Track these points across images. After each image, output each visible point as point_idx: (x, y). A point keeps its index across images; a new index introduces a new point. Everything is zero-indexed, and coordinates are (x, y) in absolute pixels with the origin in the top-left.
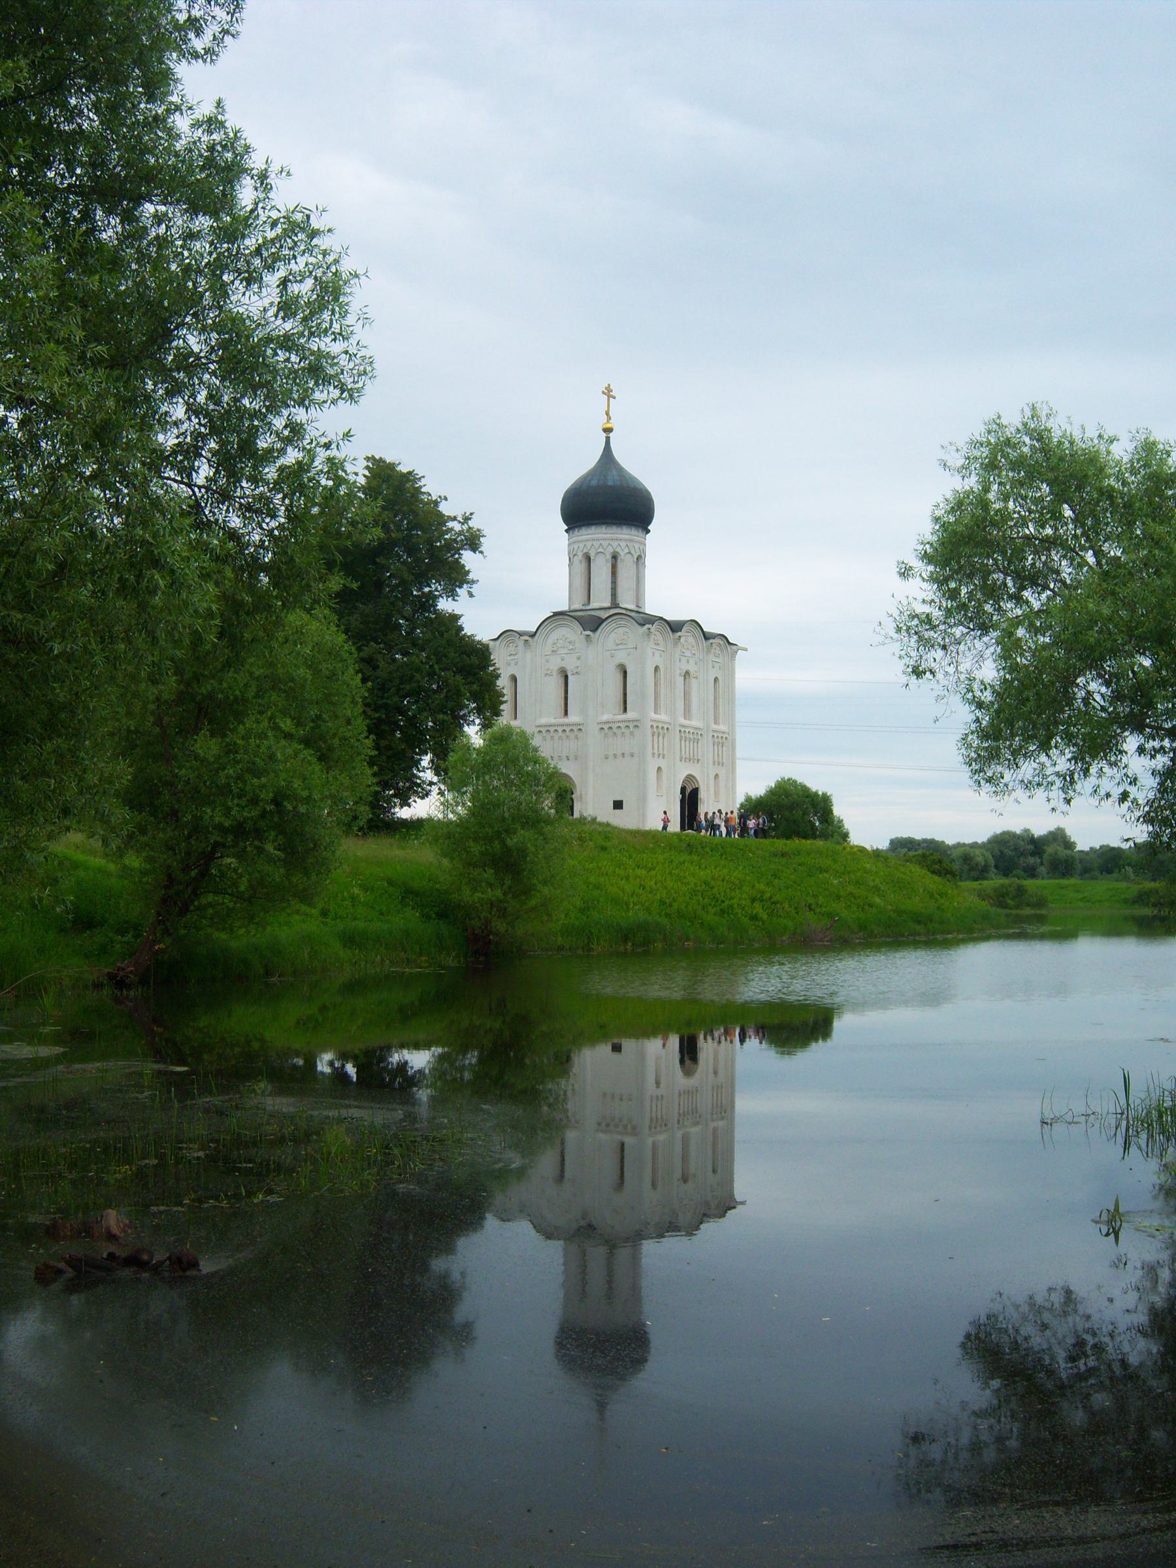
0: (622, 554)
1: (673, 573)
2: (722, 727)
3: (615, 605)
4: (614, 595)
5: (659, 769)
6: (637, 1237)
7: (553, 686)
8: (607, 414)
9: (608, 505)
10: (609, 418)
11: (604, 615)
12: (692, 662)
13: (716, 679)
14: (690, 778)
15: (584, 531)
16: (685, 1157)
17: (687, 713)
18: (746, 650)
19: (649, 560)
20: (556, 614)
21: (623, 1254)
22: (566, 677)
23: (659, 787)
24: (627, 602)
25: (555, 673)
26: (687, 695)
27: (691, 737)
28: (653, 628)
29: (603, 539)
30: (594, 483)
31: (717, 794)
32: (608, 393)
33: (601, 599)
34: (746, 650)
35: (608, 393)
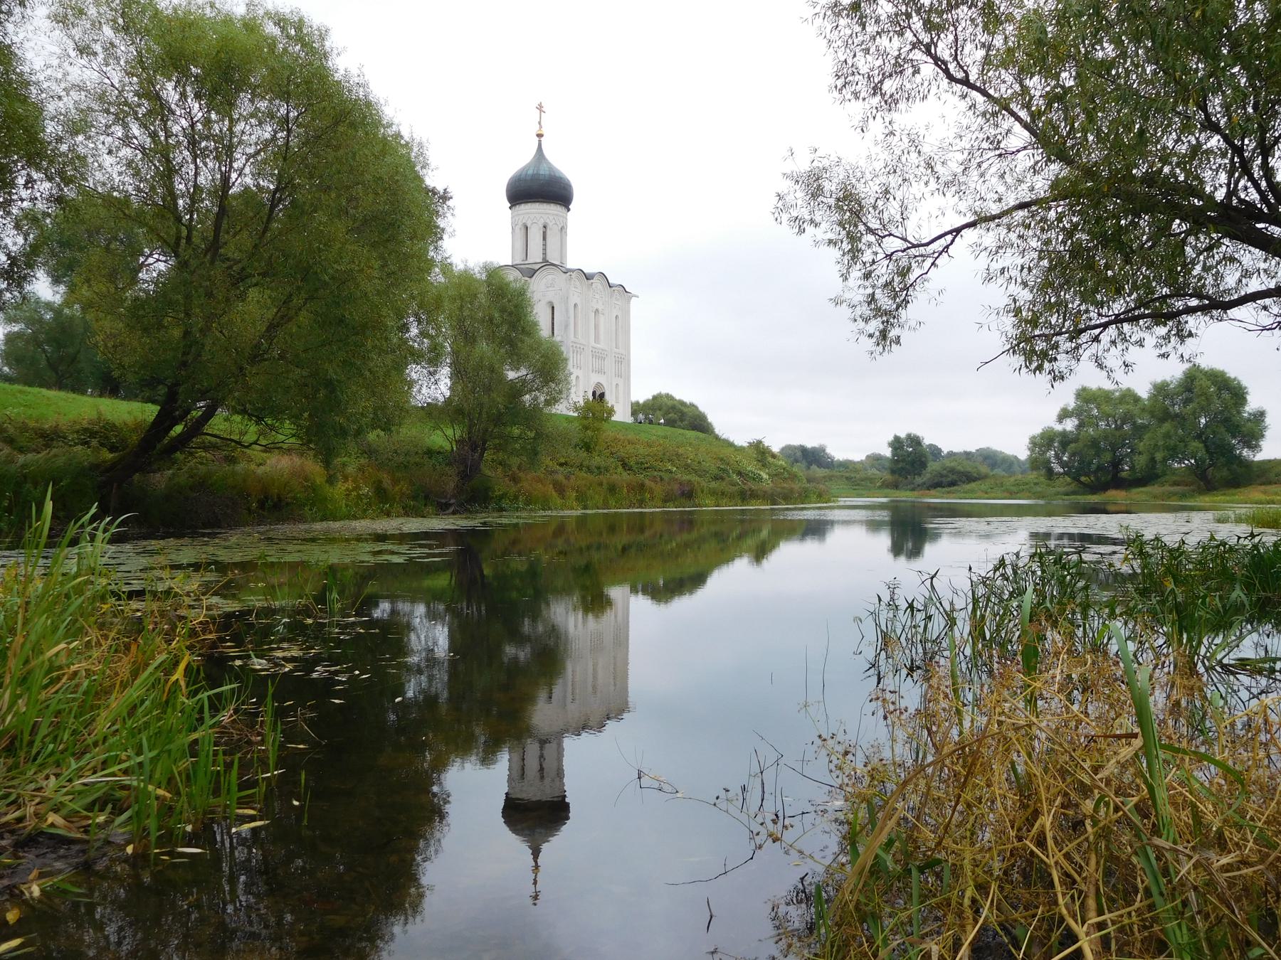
0: (550, 225)
1: (587, 237)
3: (545, 260)
4: (545, 254)
6: (559, 735)
9: (539, 190)
11: (537, 267)
14: (599, 385)
15: (523, 206)
16: (595, 677)
17: (597, 339)
19: (569, 231)
21: (550, 749)
26: (596, 327)
27: (599, 356)
28: (574, 275)
29: (536, 212)
30: (530, 172)
32: (540, 108)
33: (535, 256)
35: (540, 108)
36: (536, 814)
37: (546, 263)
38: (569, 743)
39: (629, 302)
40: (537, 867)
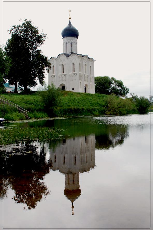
0: (73, 42)
1: (83, 46)
2: (92, 75)
5: (81, 82)
7: (61, 67)
8: (70, 15)
9: (71, 33)
10: (70, 16)
11: (69, 54)
12: (86, 63)
13: (91, 66)
15: (66, 38)
17: (86, 72)
18: (96, 61)
20: (60, 54)
21: (76, 176)
22: (63, 66)
23: (81, 86)
24: (74, 51)
25: (61, 65)
27: (86, 77)
28: (79, 56)
29: (70, 39)
31: (91, 87)
32: (70, 11)
33: (69, 51)
34: (96, 61)
35: (70, 11)
36: (72, 192)
37: (72, 53)
38: (80, 175)
39: (94, 62)
40: (73, 207)
